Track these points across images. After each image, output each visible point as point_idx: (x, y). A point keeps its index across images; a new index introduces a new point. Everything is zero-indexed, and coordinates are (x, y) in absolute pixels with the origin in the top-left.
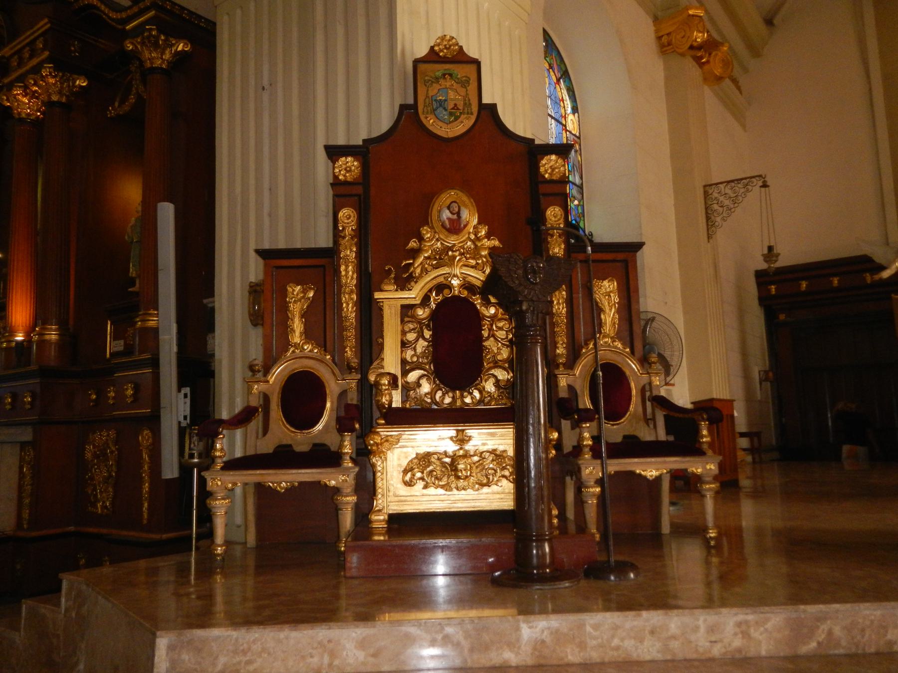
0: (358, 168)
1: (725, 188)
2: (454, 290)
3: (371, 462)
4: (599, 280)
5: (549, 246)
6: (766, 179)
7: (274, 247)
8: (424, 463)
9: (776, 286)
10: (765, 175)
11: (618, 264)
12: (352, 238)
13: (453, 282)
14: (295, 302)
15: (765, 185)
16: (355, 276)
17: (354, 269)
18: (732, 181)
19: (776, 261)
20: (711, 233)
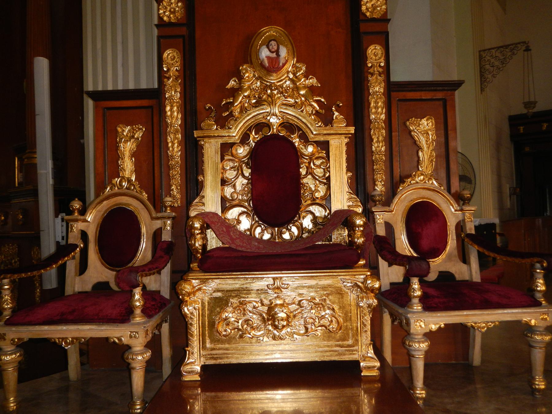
0: (182, 9)
1: (496, 52)
2: (273, 129)
3: (183, 313)
4: (417, 118)
5: (369, 85)
6: (529, 45)
7: (104, 89)
8: (239, 311)
9: (523, 127)
10: (528, 41)
11: (437, 103)
12: (176, 79)
13: (272, 120)
14: (126, 142)
15: (528, 49)
16: (180, 116)
17: (178, 109)
18: (502, 47)
19: (534, 107)
20: (483, 87)
